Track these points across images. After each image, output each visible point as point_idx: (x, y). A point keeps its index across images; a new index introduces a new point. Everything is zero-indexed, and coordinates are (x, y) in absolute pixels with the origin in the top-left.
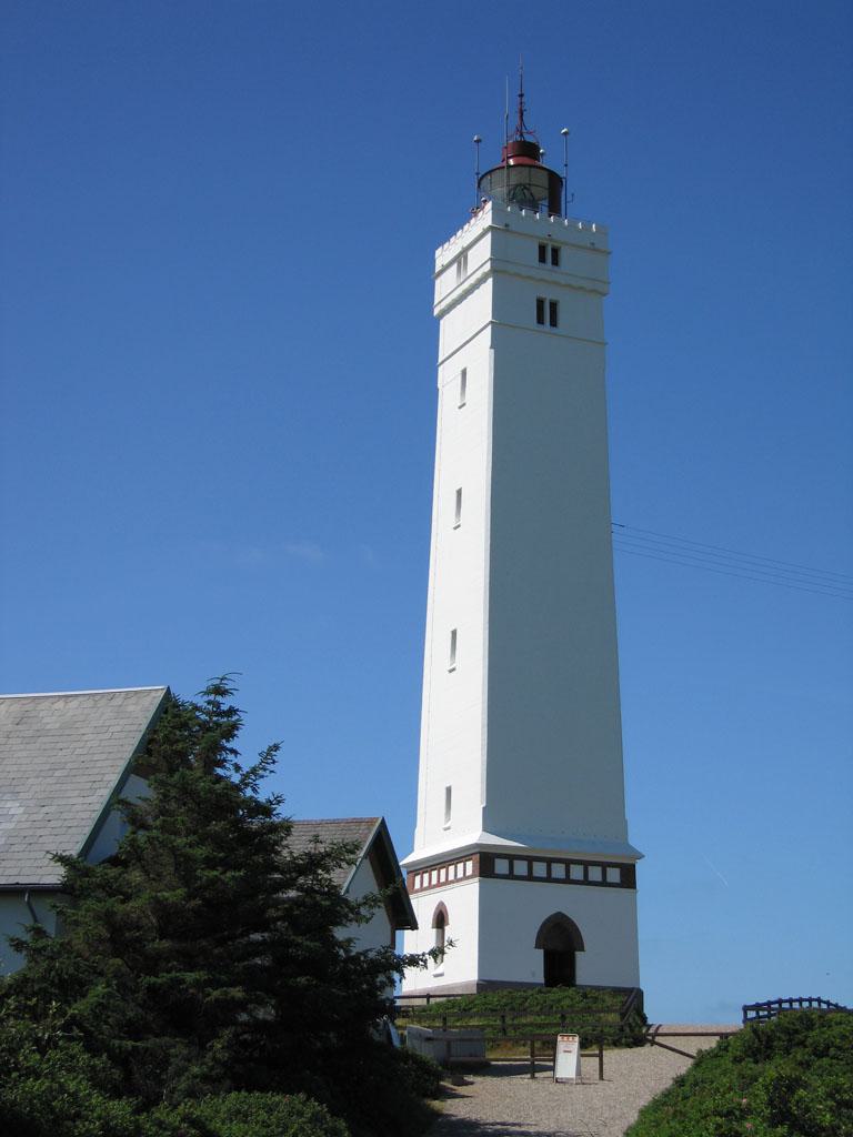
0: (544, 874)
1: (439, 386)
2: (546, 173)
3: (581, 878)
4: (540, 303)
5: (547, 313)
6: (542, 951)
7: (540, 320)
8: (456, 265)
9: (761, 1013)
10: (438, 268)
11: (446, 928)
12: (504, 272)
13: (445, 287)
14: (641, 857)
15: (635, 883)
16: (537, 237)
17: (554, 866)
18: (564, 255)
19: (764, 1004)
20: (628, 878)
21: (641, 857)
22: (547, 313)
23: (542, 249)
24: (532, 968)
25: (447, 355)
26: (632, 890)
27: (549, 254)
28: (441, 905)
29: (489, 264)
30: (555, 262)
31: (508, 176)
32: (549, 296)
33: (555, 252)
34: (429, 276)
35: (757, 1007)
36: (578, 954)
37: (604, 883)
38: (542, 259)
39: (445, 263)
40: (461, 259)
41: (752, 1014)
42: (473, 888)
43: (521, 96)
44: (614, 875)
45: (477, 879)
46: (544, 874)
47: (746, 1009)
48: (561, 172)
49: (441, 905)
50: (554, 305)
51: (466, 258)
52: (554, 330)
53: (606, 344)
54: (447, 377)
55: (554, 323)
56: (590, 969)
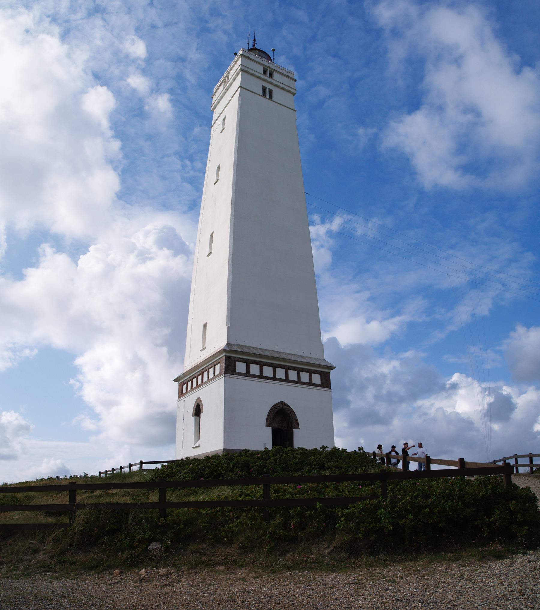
1: (211, 135)
3: (296, 379)
6: (271, 428)
11: (202, 415)
12: (247, 72)
14: (332, 368)
15: (330, 385)
18: (275, 75)
20: (326, 383)
21: (332, 368)
24: (260, 439)
27: (268, 72)
28: (199, 399)
32: (269, 86)
36: (295, 431)
37: (311, 384)
42: (221, 382)
44: (317, 379)
49: (199, 399)
55: (271, 97)
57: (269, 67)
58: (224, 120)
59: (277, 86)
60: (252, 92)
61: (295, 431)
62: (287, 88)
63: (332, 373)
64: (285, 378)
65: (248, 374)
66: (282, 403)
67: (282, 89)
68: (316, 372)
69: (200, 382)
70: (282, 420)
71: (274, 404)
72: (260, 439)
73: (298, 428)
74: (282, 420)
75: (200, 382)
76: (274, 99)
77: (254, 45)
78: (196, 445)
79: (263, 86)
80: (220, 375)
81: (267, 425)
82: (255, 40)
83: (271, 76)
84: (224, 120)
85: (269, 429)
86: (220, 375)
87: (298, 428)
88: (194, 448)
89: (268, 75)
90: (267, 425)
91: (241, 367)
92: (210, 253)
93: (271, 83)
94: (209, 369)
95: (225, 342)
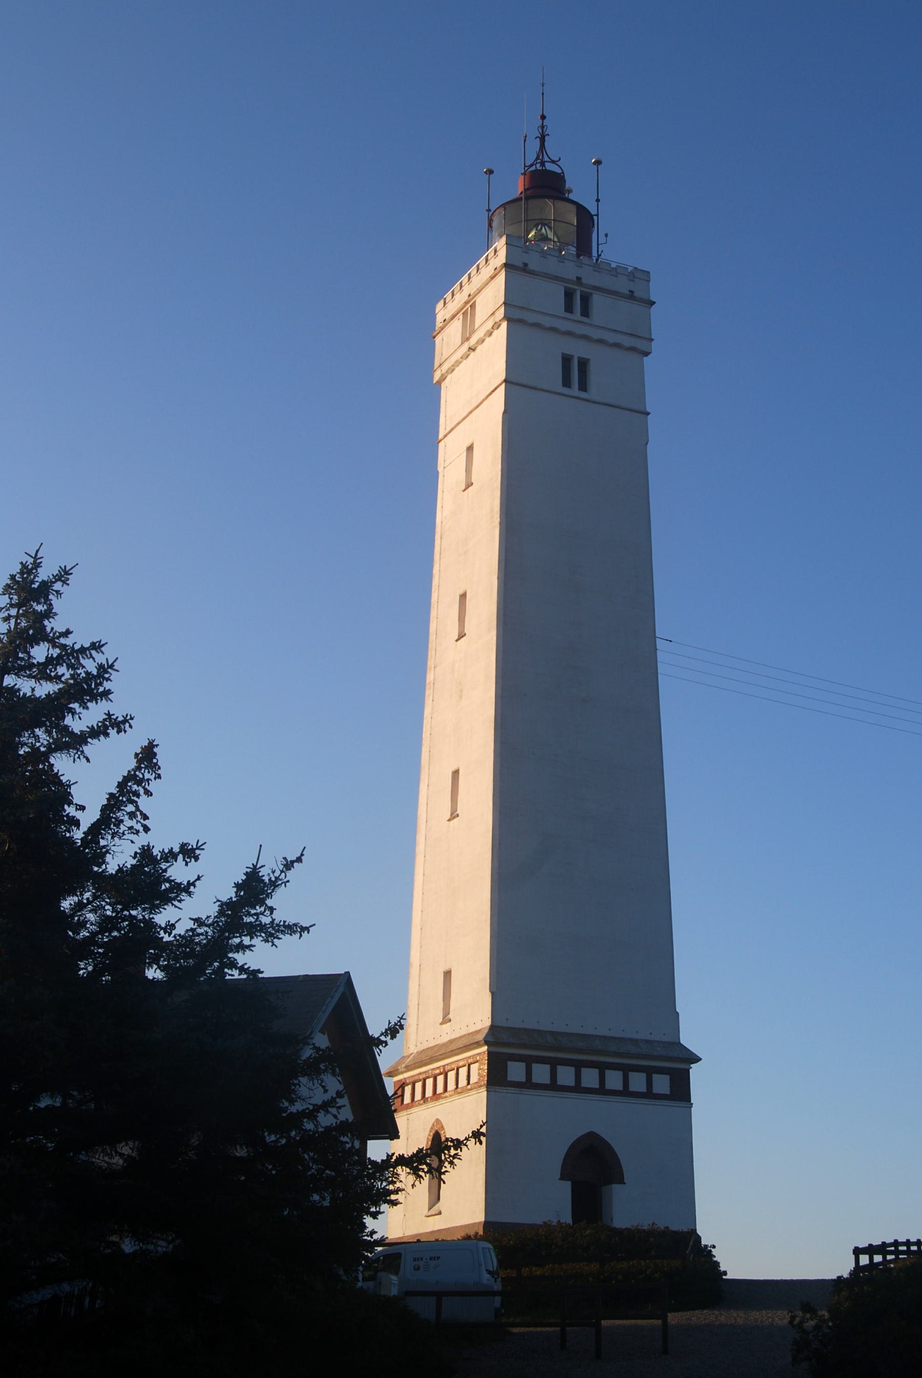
0: (571, 1082)
1: (440, 469)
2: (573, 208)
4: (566, 360)
5: (576, 373)
6: (569, 1183)
7: (567, 383)
8: (460, 316)
9: (889, 1257)
10: (439, 324)
12: (521, 321)
13: (448, 341)
14: (697, 1059)
16: (562, 280)
17: (584, 1071)
18: (597, 300)
19: (891, 1245)
20: (680, 1091)
21: (697, 1059)
22: (576, 373)
23: (569, 296)
24: (552, 1204)
25: (448, 429)
26: (682, 1104)
27: (578, 300)
29: (502, 310)
30: (585, 312)
31: (526, 210)
32: (578, 350)
33: (586, 299)
34: (427, 333)
35: (871, 1250)
37: (649, 1094)
38: (569, 308)
39: (447, 317)
40: (468, 310)
41: (864, 1260)
43: (543, 117)
44: (662, 1084)
45: (484, 1089)
46: (571, 1082)
47: (857, 1252)
48: (593, 212)
50: (583, 364)
51: (473, 307)
52: (583, 395)
53: (648, 414)
54: (449, 455)
55: (583, 386)
56: (627, 1209)
61: (616, 1187)
62: (627, 342)
63: (695, 1071)
64: (597, 1086)
65: (528, 1084)
66: (591, 1135)
67: (617, 345)
68: (661, 1071)
69: (440, 1089)
70: (592, 1166)
71: (576, 1137)
72: (552, 1204)
73: (622, 1182)
74: (592, 1166)
75: (440, 1089)
76: (594, 392)
79: (563, 354)
80: (478, 1086)
81: (563, 1178)
85: (568, 1185)
86: (478, 1086)
87: (622, 1182)
90: (563, 1178)
91: (516, 1071)
95: (488, 1023)
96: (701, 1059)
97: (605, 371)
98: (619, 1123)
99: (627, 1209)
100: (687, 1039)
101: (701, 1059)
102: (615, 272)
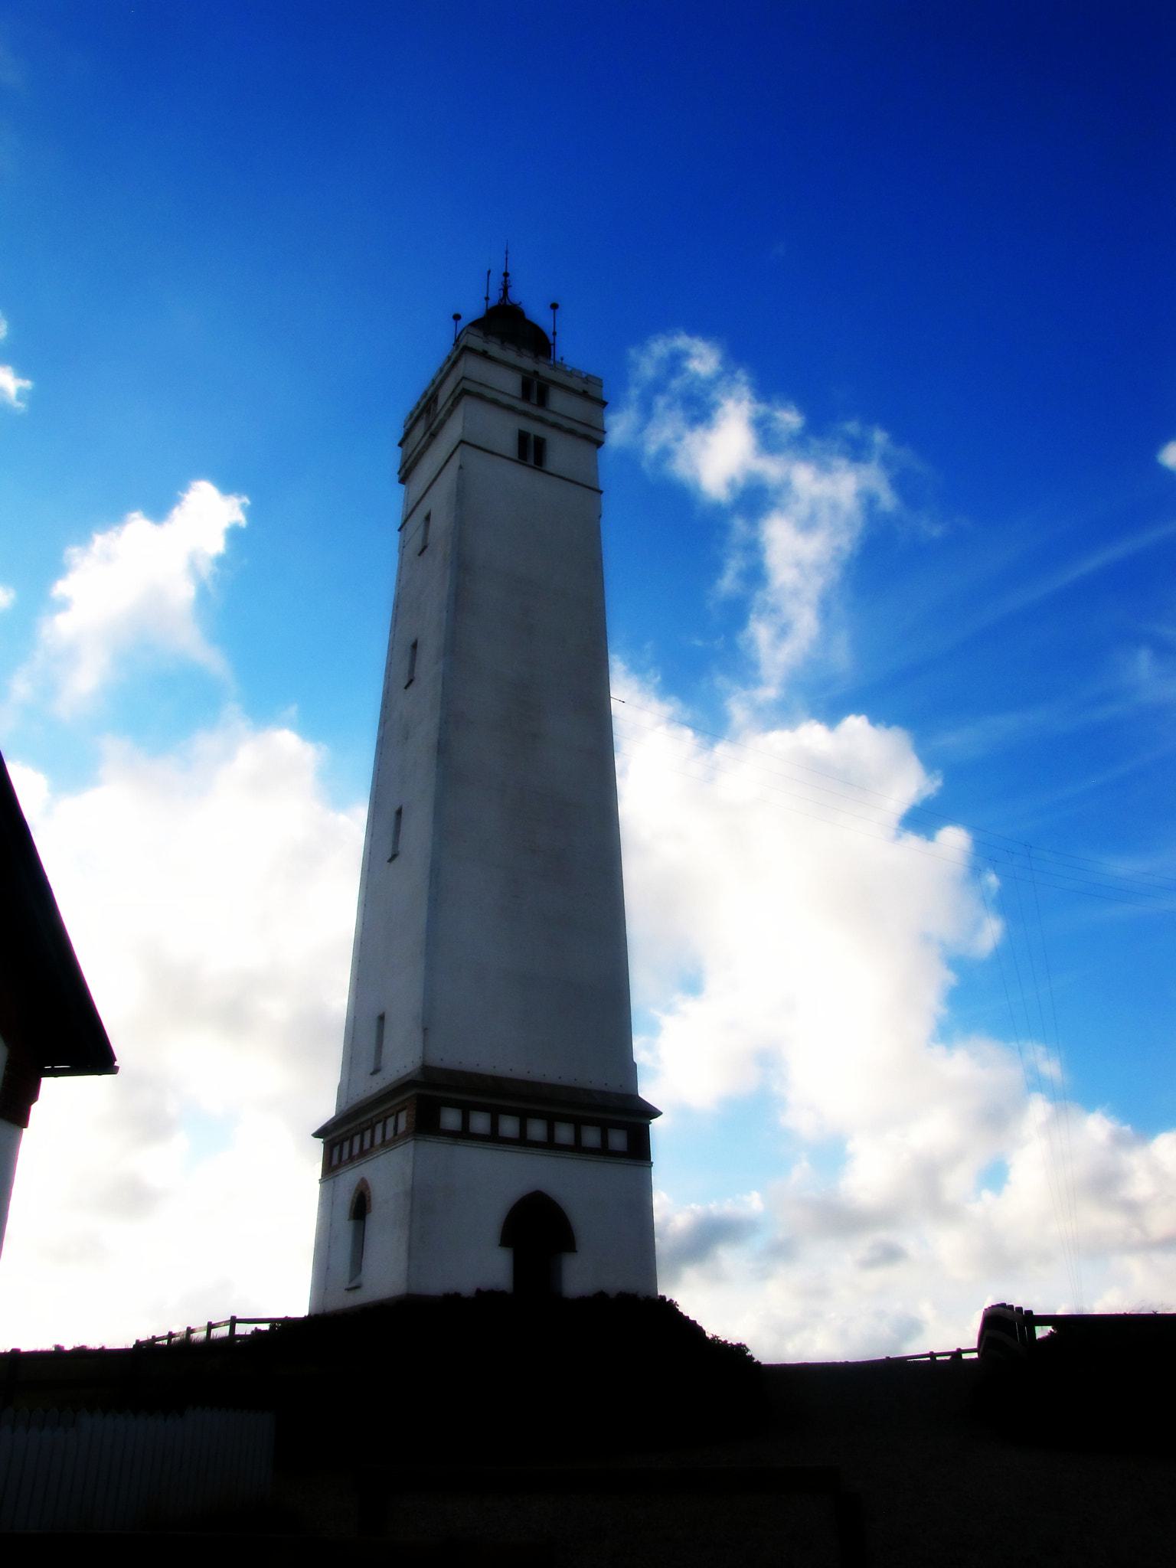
20: (639, 1151)
27: (535, 390)
32: (535, 429)
44: (618, 1140)
56: (580, 1276)
57: (536, 373)
58: (428, 518)
59: (555, 426)
60: (492, 453)
65: (464, 1134)
67: (571, 432)
68: (618, 1125)
69: (367, 1145)
75: (367, 1145)
77: (505, 289)
78: (353, 1285)
82: (506, 275)
83: (542, 402)
84: (428, 518)
88: (348, 1290)
89: (534, 400)
91: (451, 1119)
92: (394, 857)
93: (541, 420)
94: (386, 1118)
96: (660, 1113)
97: (561, 452)
98: (568, 1181)
99: (580, 1276)
100: (647, 1092)
101: (660, 1113)
102: (571, 374)
